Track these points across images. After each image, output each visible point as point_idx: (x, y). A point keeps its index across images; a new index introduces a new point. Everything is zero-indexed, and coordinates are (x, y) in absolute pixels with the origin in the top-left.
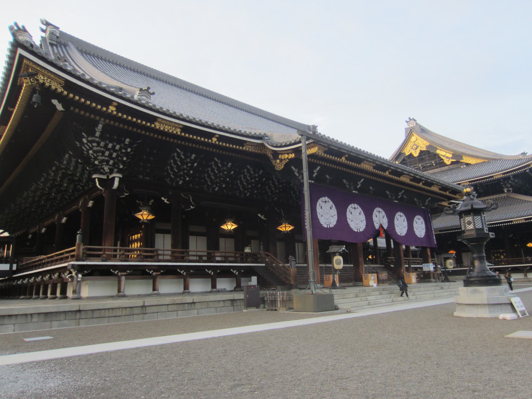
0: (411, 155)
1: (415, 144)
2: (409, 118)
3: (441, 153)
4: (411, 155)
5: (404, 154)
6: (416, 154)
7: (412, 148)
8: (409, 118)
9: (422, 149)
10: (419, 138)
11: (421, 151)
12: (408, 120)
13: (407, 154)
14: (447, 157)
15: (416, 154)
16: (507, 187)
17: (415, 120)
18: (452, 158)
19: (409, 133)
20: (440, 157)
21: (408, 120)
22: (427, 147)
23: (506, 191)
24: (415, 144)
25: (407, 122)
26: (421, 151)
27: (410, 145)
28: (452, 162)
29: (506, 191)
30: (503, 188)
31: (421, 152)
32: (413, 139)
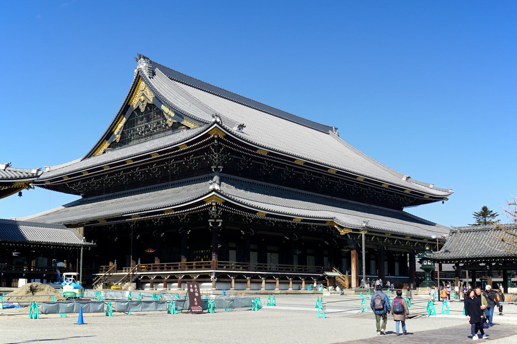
6: (143, 110)
11: (147, 103)
13: (135, 107)
15: (143, 110)
23: (213, 170)
26: (147, 103)
29: (213, 170)
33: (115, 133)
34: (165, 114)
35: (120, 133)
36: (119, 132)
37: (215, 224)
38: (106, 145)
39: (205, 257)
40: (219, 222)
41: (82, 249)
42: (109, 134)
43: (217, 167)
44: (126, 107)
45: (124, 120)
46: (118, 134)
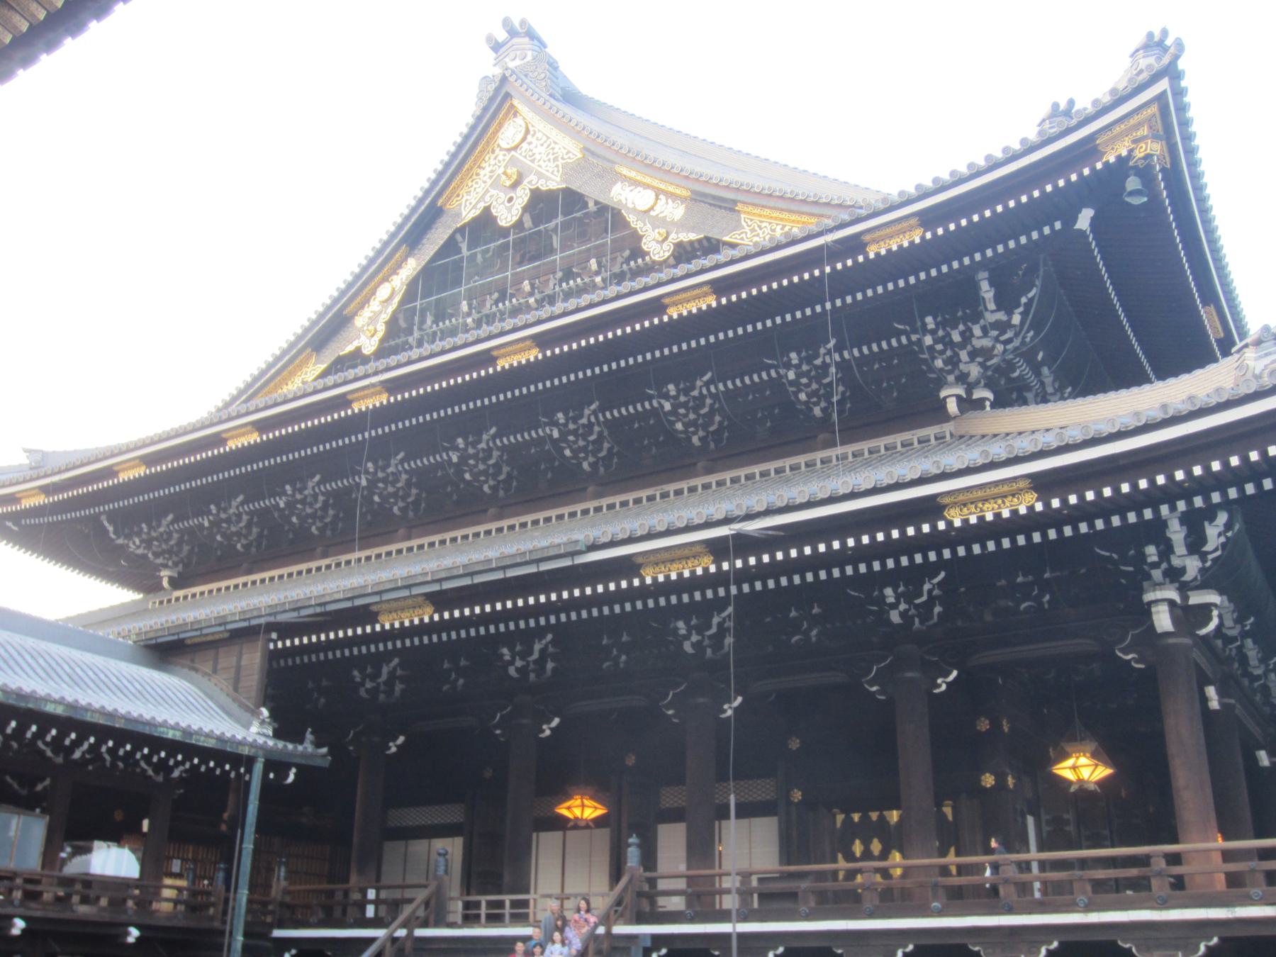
0: (485, 222)
1: (513, 162)
2: (507, 23)
3: (631, 198)
4: (485, 222)
5: (459, 215)
6: (507, 216)
7: (496, 184)
8: (507, 23)
9: (545, 186)
10: (538, 123)
12: (502, 36)
13: (468, 213)
14: (658, 222)
16: (962, 378)
17: (531, 35)
18: (681, 225)
19: (497, 104)
20: (626, 224)
21: (502, 36)
22: (569, 170)
24: (513, 162)
25: (496, 47)
27: (492, 167)
28: (679, 245)
30: (940, 383)
31: (541, 204)
32: (509, 133)
33: (359, 321)
34: (631, 218)
35: (386, 317)
36: (376, 316)
37: (1188, 616)
38: (312, 370)
39: (858, 848)
40: (1206, 609)
41: (258, 767)
42: (335, 323)
43: (969, 391)
44: (427, 216)
45: (411, 267)
46: (373, 319)
